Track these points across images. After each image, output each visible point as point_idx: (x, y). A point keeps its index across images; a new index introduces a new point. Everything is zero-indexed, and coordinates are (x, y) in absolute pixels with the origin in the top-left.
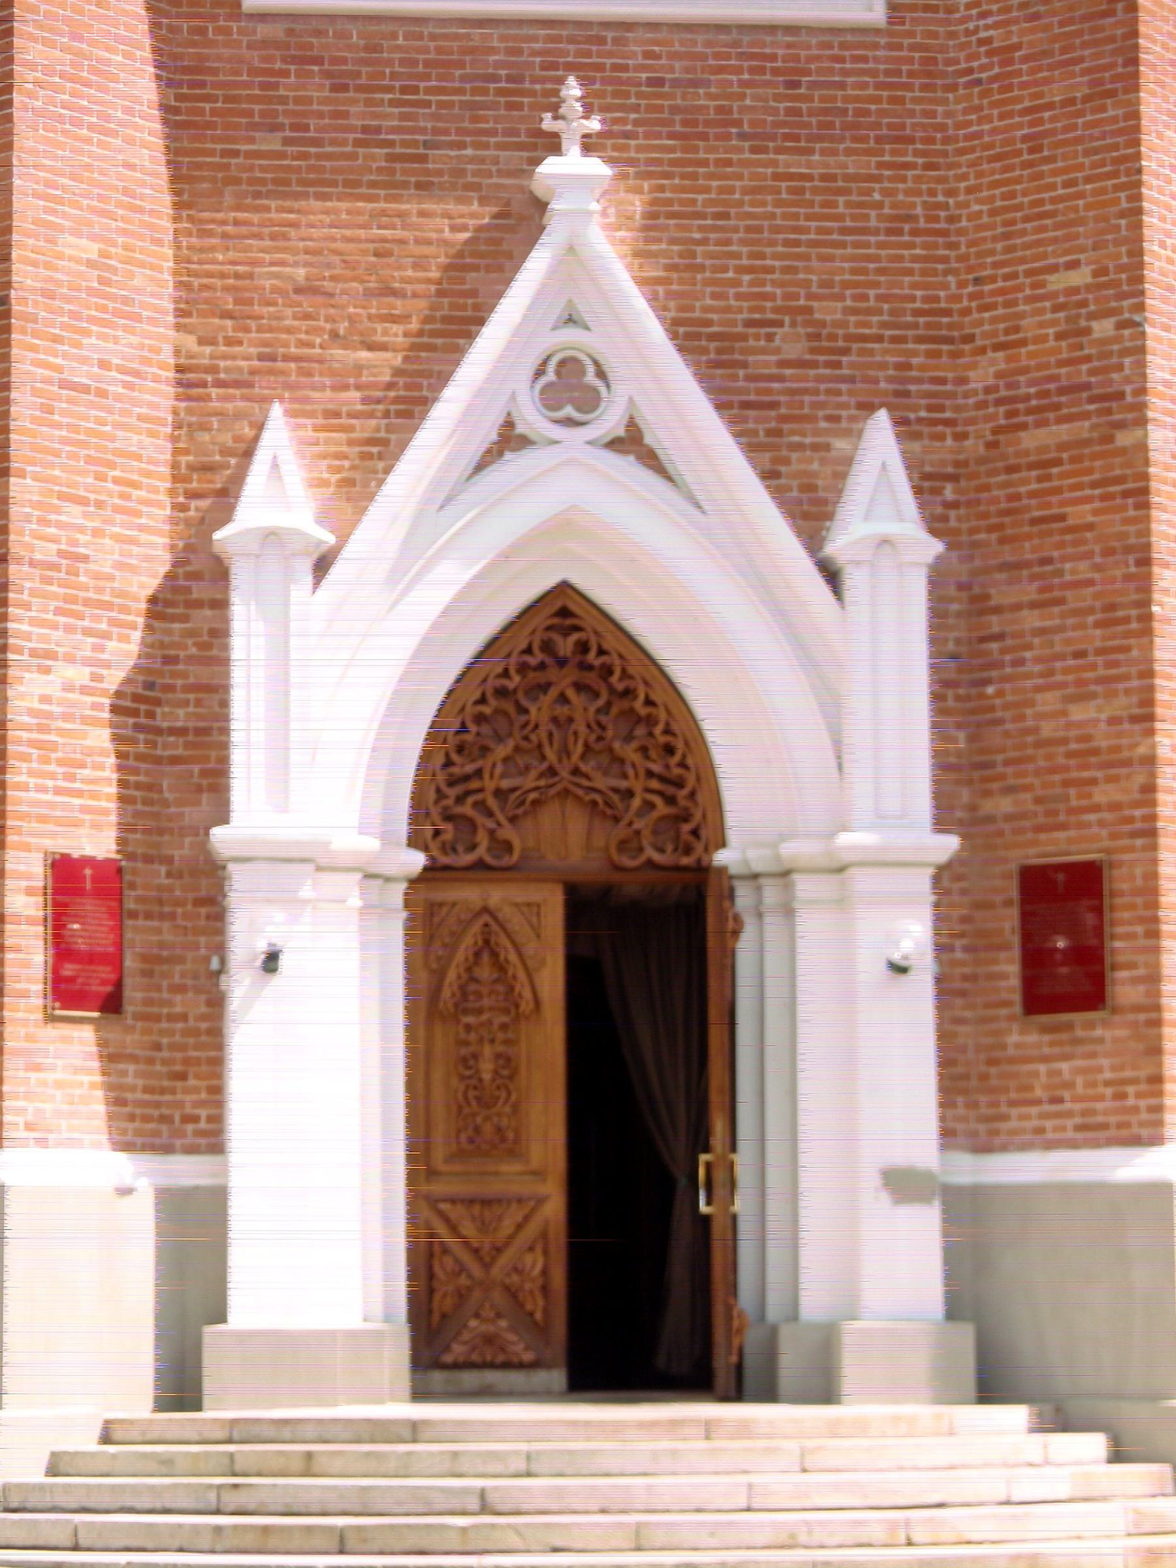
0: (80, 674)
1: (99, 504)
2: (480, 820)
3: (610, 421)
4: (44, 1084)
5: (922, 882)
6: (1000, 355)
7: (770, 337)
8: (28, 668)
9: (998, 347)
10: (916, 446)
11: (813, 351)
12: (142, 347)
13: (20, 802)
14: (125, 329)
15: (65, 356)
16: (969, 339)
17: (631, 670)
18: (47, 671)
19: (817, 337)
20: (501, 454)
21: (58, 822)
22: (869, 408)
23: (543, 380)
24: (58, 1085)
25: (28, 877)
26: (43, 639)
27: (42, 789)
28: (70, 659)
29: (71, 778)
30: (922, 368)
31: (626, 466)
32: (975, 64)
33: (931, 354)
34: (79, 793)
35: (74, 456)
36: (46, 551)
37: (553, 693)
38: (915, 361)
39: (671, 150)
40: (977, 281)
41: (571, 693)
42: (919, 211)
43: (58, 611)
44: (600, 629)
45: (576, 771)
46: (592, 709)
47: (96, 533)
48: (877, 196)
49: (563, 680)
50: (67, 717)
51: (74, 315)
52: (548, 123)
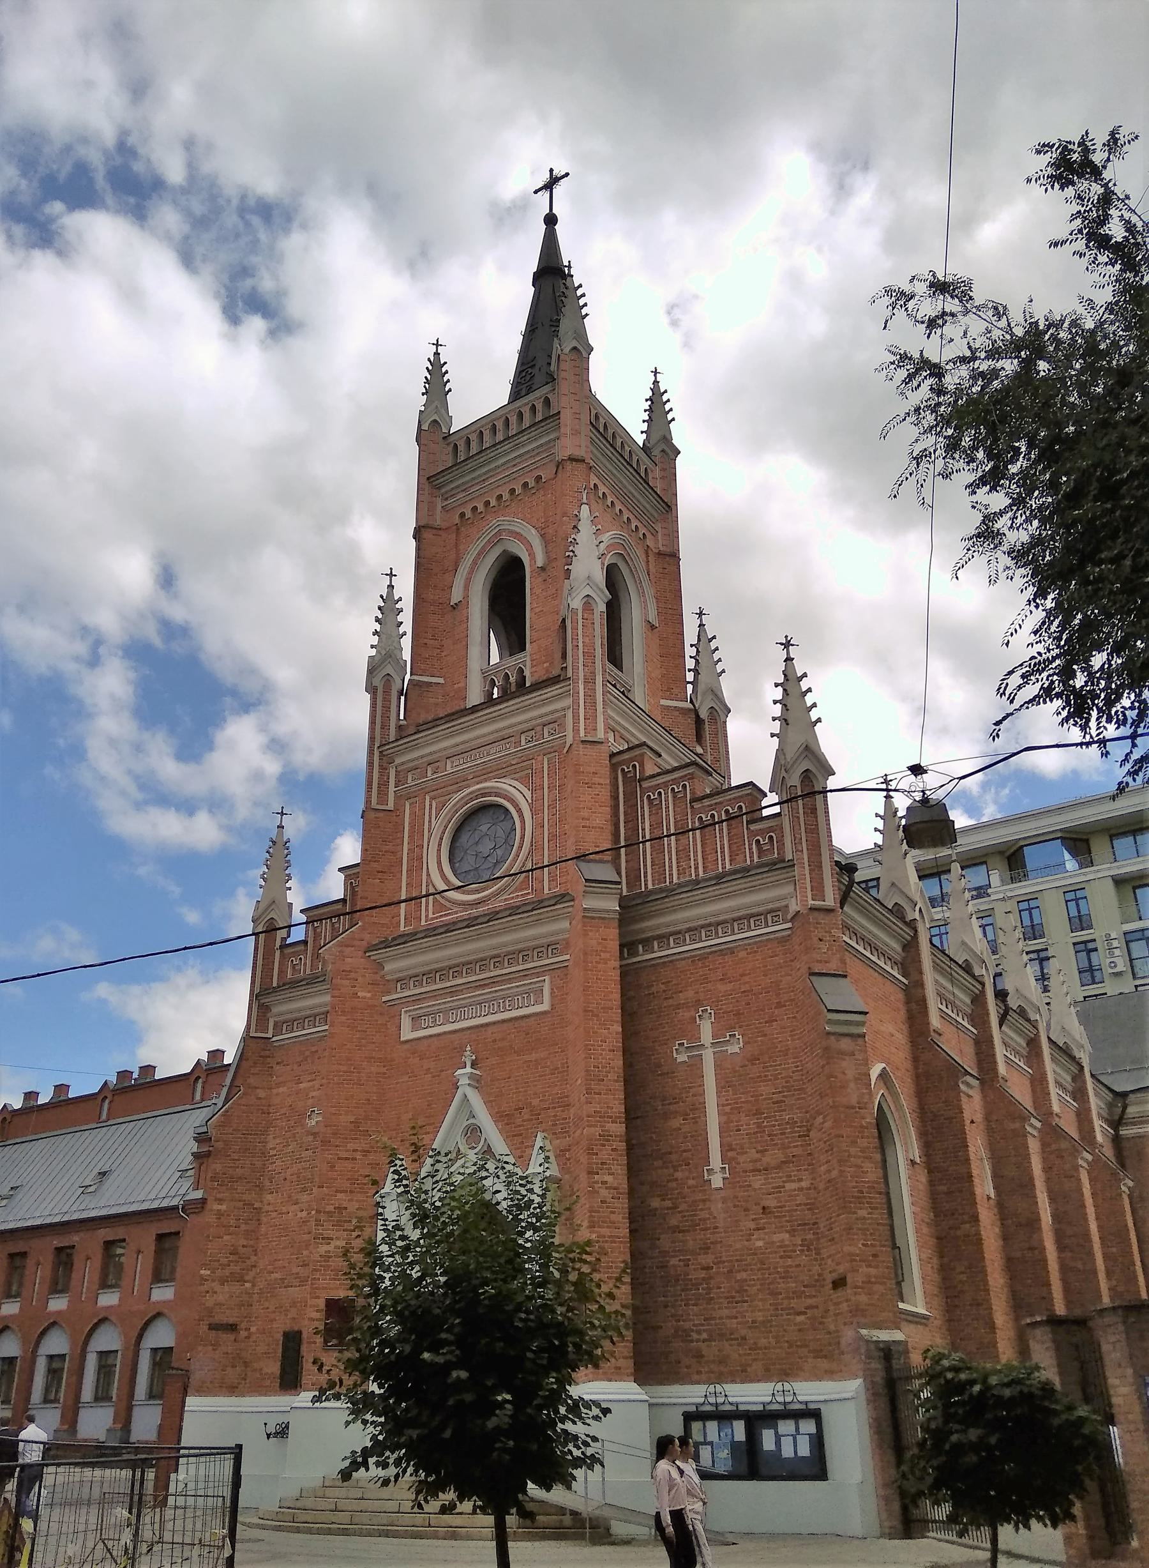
7: (520, 1113)
11: (532, 1115)
28: (337, 1238)
33: (563, 1111)
36: (331, 1208)
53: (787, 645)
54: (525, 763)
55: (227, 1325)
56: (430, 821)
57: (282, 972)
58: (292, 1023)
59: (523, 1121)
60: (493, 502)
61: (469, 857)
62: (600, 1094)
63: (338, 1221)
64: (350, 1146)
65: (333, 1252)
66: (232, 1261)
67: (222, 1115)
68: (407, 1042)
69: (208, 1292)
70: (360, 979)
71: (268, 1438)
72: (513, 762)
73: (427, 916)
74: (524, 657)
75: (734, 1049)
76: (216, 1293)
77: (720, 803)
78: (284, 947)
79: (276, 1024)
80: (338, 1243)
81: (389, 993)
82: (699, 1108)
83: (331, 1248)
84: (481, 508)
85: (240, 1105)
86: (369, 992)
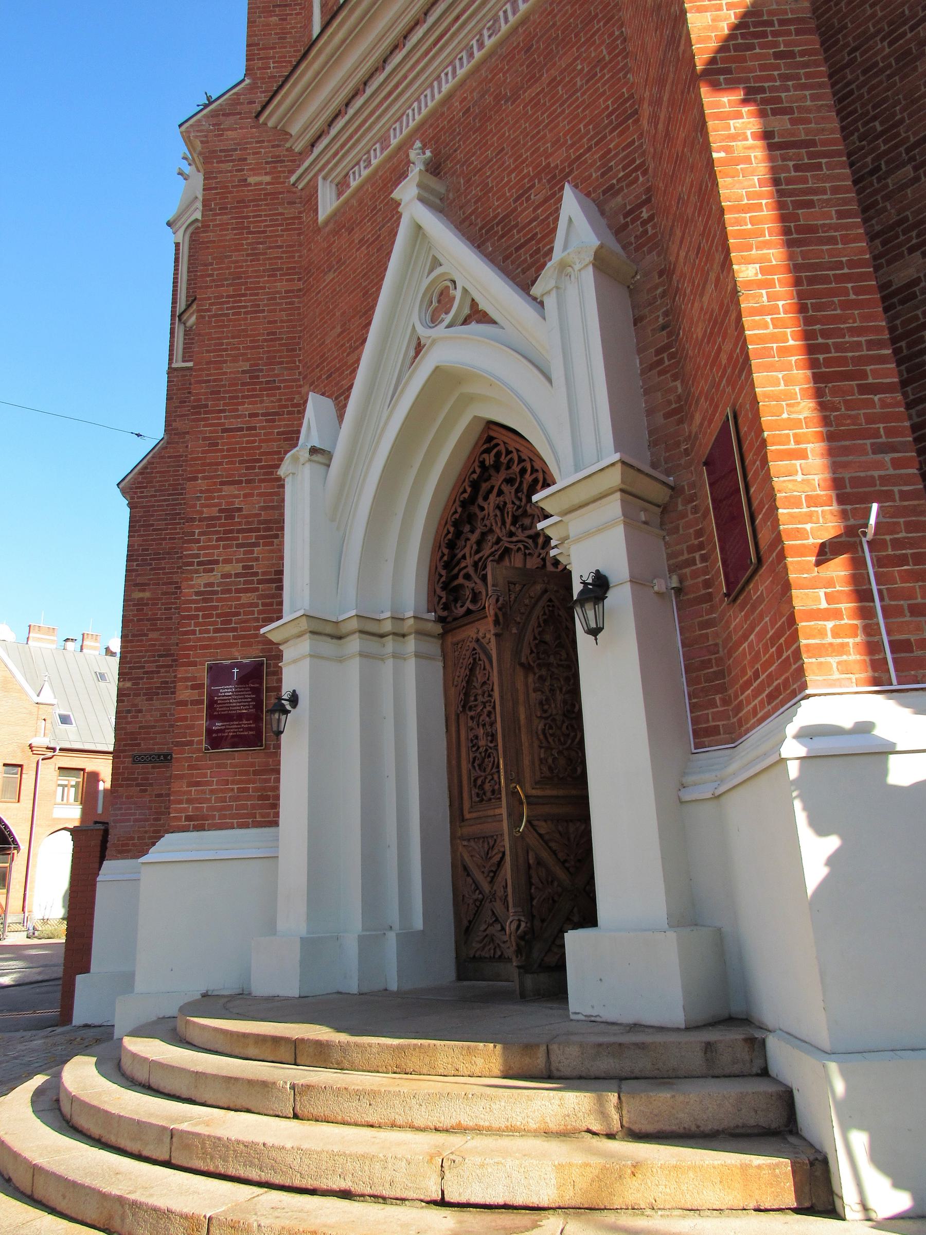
0: (238, 568)
1: (248, 482)
2: (466, 583)
4: (204, 792)
7: (528, 199)
8: (197, 572)
10: (619, 199)
12: (280, 400)
13: (189, 640)
14: (268, 395)
15: (225, 417)
17: (524, 457)
18: (212, 570)
19: (554, 177)
21: (217, 647)
24: (212, 791)
25: (194, 678)
26: (206, 555)
27: (208, 631)
28: (227, 561)
29: (230, 622)
30: (616, 147)
34: (234, 630)
35: (233, 463)
36: (214, 512)
37: (495, 491)
39: (475, 139)
41: (505, 488)
42: (605, 52)
43: (218, 540)
44: (506, 441)
45: (511, 534)
46: (513, 491)
47: (245, 496)
49: (498, 480)
50: (223, 592)
51: (231, 398)
55: (159, 756)
59: (535, 210)
63: (225, 532)
64: (246, 408)
65: (219, 585)
66: (162, 666)
67: (141, 473)
68: (327, 223)
69: (129, 712)
70: (251, 160)
76: (140, 711)
80: (228, 568)
83: (215, 577)
85: (162, 457)
86: (266, 174)
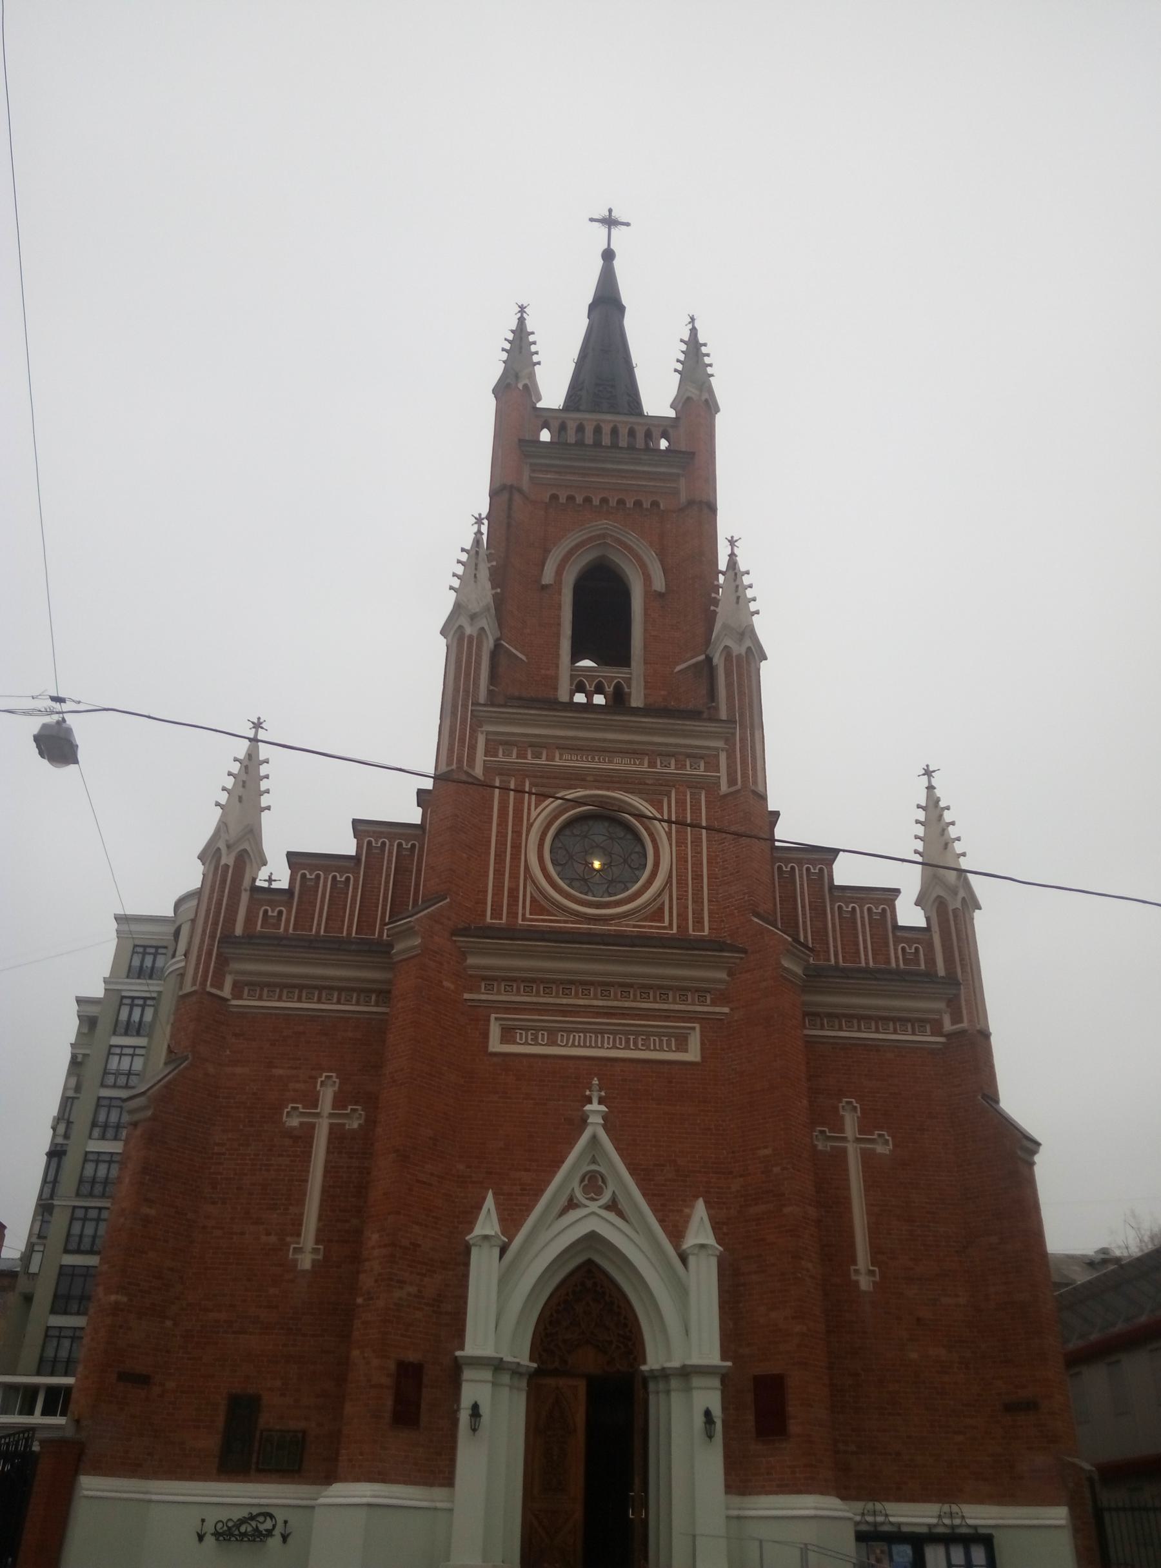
0: (413, 1290)
3: (606, 1198)
5: (716, 1382)
6: (742, 1179)
9: (741, 1176)
16: (731, 1173)
18: (401, 1288)
20: (568, 1211)
22: (696, 1197)
23: (583, 1184)
31: (611, 1216)
32: (731, 1077)
38: (712, 1180)
40: (733, 1152)
48: (699, 1121)
52: (588, 1093)
53: (928, 773)
54: (662, 788)
56: (529, 809)
57: (250, 920)
58: (257, 986)
60: (596, 502)
61: (576, 865)
62: (799, 1171)
67: (166, 1086)
69: (121, 1327)
71: (201, 1537)
72: (647, 782)
73: (524, 915)
74: (630, 674)
75: (880, 1149)
77: (862, 899)
78: (255, 890)
79: (235, 985)
81: (471, 991)
82: (848, 1200)
84: (579, 499)
